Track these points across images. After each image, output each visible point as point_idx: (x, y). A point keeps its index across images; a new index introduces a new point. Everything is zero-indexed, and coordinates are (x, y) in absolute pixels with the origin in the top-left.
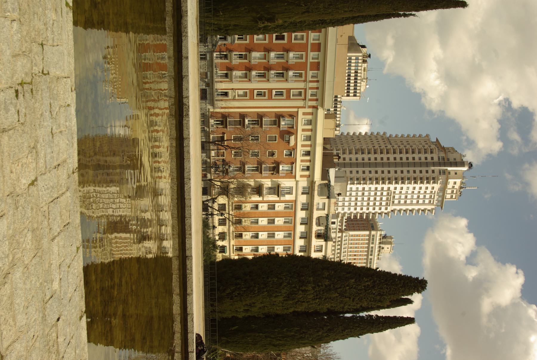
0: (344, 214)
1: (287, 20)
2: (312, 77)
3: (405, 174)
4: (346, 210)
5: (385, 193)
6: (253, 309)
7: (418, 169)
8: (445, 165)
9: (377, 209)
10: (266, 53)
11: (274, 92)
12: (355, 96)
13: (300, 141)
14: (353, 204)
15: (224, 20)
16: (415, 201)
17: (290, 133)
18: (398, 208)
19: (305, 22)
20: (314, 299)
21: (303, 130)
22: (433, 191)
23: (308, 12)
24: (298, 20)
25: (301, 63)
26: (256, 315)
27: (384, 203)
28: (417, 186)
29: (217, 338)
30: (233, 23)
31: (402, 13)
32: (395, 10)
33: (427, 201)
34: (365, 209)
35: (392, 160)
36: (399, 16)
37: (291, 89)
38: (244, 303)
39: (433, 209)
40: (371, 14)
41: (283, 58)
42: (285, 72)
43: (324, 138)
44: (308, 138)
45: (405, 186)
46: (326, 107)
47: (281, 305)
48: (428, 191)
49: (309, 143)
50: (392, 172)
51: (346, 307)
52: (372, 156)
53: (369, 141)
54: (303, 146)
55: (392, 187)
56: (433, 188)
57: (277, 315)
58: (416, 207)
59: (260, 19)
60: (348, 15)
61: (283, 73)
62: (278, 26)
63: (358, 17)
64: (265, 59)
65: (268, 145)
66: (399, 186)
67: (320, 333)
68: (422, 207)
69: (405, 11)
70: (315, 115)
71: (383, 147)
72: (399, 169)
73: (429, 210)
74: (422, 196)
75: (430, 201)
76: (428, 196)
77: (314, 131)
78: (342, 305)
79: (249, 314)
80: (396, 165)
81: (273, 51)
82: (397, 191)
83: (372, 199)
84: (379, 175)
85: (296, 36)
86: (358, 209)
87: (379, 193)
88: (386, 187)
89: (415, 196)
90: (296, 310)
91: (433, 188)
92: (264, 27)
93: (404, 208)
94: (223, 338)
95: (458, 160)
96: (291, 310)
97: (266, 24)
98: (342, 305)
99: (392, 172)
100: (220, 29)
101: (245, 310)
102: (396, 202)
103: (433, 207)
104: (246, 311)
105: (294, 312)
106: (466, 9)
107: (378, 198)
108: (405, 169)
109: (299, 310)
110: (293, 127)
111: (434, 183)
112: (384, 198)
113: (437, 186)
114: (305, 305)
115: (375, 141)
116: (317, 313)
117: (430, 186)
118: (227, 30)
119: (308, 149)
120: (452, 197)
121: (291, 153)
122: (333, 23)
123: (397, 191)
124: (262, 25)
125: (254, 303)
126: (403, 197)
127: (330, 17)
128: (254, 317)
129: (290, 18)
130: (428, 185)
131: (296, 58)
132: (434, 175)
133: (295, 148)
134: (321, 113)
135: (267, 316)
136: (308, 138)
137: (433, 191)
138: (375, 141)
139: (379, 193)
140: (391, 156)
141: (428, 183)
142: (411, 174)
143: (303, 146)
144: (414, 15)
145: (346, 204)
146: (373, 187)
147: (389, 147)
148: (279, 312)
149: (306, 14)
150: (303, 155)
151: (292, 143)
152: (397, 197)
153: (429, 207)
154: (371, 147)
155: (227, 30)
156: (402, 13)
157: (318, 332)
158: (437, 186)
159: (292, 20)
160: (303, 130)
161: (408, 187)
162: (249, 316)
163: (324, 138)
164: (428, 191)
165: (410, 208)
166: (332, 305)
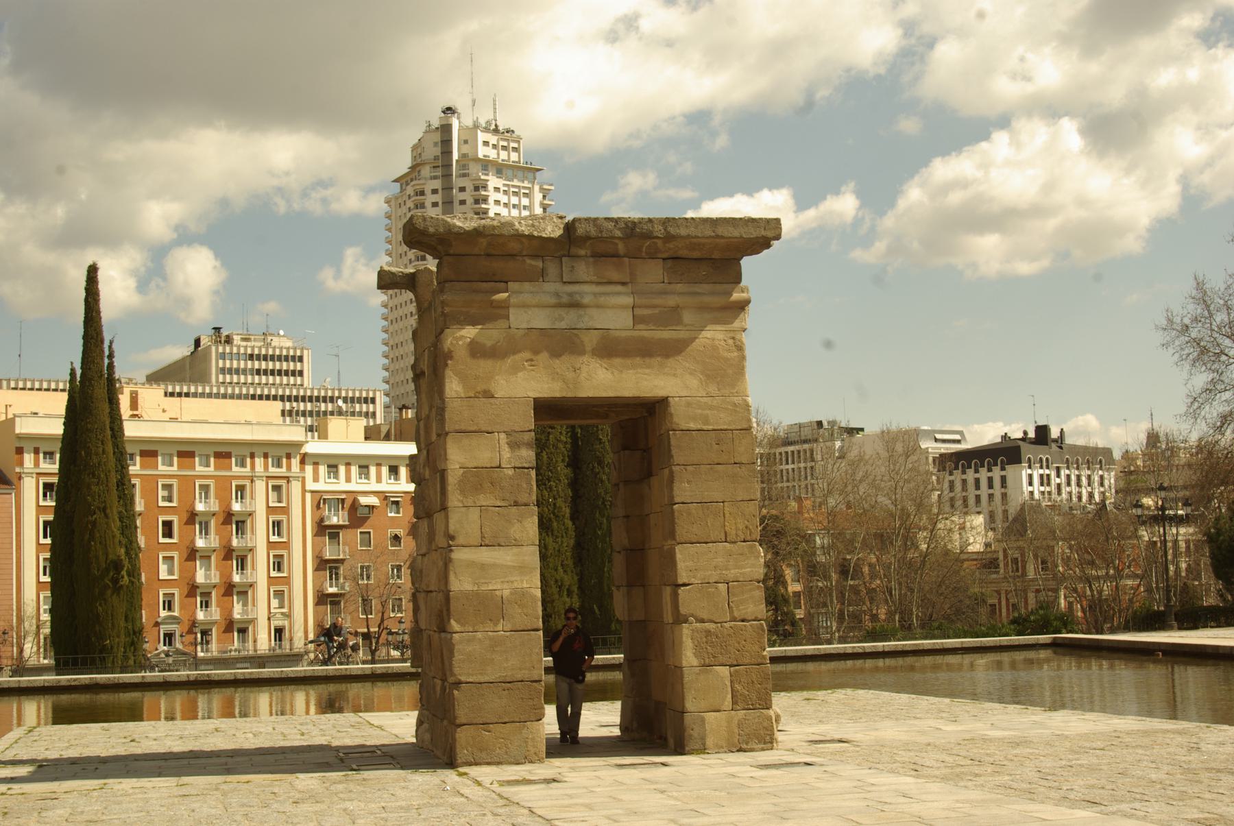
1: (117, 541)
2: (243, 465)
6: (567, 583)
8: (448, 166)
10: (198, 555)
11: (274, 539)
12: (301, 359)
15: (118, 637)
17: (355, 506)
19: (120, 513)
20: (550, 488)
21: (348, 480)
22: (503, 188)
23: (104, 509)
24: (118, 523)
25: (216, 488)
26: (576, 578)
29: (611, 638)
30: (122, 624)
31: (106, 361)
32: (102, 375)
33: (525, 202)
36: (111, 366)
37: (268, 507)
38: (556, 596)
39: (541, 189)
40: (108, 410)
41: (207, 524)
42: (234, 519)
43: (366, 438)
44: (364, 469)
46: (302, 438)
47: (559, 540)
48: (504, 199)
49: (373, 470)
51: (563, 438)
53: (401, 324)
54: (379, 480)
56: (497, 189)
57: (579, 546)
59: (115, 581)
60: (110, 448)
61: (237, 523)
62: (127, 553)
63: (112, 429)
64: (209, 557)
65: (376, 548)
67: (604, 477)
69: (103, 359)
70: (316, 460)
73: (544, 197)
75: (526, 195)
76: (514, 200)
77: (348, 460)
78: (561, 446)
79: (575, 589)
81: (193, 542)
85: (164, 499)
90: (568, 515)
91: (497, 189)
92: (129, 575)
94: (613, 627)
96: (569, 523)
97: (124, 573)
98: (561, 446)
100: (133, 643)
101: (568, 595)
103: (537, 188)
104: (570, 593)
105: (572, 518)
106: (100, 265)
109: (568, 511)
110: (343, 500)
111: (485, 187)
113: (493, 181)
114: (560, 502)
115: (400, 312)
116: (574, 484)
117: (493, 196)
118: (134, 633)
119: (385, 470)
120: (515, 149)
121: (393, 502)
122: (123, 467)
124: (126, 578)
125: (556, 581)
127: (113, 473)
128: (580, 580)
129: (114, 537)
130: (491, 200)
131: (206, 497)
132: (469, 186)
133: (384, 496)
134: (314, 447)
135: (579, 560)
136: (364, 469)
137: (503, 188)
138: (400, 312)
141: (485, 200)
143: (379, 480)
144: (111, 342)
148: (572, 542)
149: (108, 511)
150: (397, 479)
151: (373, 501)
153: (538, 197)
155: (134, 633)
156: (106, 361)
157: (602, 481)
158: (493, 181)
159: (117, 533)
160: (348, 480)
162: (579, 588)
163: (366, 438)
164: (504, 199)
166: (560, 460)
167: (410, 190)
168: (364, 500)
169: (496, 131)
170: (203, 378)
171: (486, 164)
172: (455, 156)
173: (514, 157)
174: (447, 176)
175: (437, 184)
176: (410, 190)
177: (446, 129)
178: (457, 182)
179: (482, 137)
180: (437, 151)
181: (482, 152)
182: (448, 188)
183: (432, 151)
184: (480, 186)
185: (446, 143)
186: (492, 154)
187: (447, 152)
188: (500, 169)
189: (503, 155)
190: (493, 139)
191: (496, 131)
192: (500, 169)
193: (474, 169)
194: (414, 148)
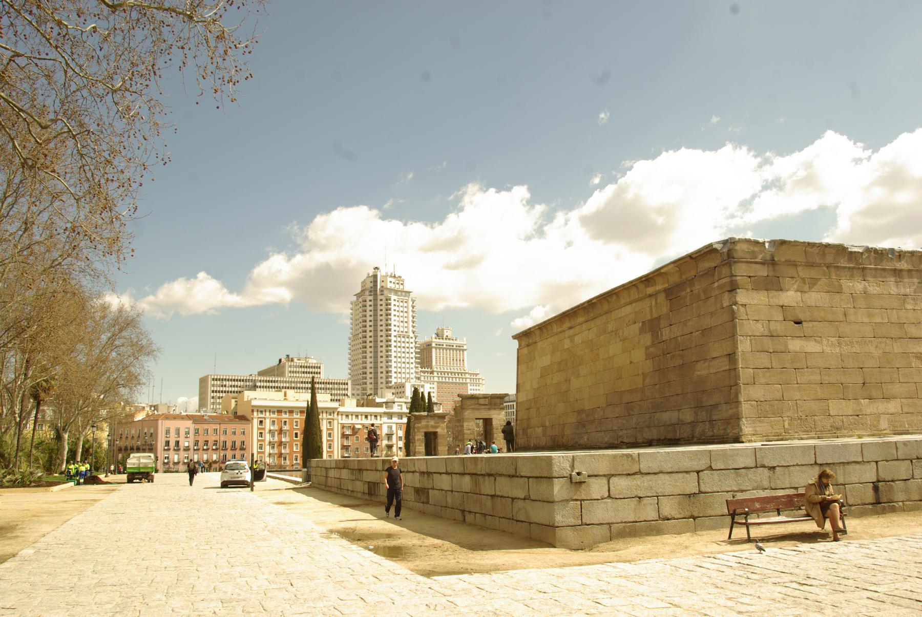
0: (416, 373)
3: (383, 323)
4: (413, 371)
5: (399, 339)
7: (379, 313)
9: (412, 345)
13: (359, 422)
14: (407, 365)
16: (406, 315)
17: (354, 428)
18: (411, 328)
27: (407, 340)
28: (393, 313)
33: (406, 305)
34: (413, 356)
35: (371, 334)
45: (393, 323)
50: (381, 333)
52: (368, 350)
55: (393, 333)
58: (411, 313)
66: (393, 328)
68: (411, 308)
71: (361, 341)
72: (379, 328)
74: (401, 309)
76: (401, 304)
80: (376, 331)
82: (397, 329)
83: (403, 350)
84: (384, 344)
86: (412, 361)
87: (399, 344)
88: (393, 339)
89: (401, 314)
93: (411, 323)
95: (372, 279)
99: (381, 333)
102: (406, 330)
107: (403, 345)
108: (379, 323)
112: (403, 340)
113: (393, 297)
117: (393, 303)
123: (397, 329)
126: (402, 324)
133: (363, 425)
139: (399, 344)
140: (369, 334)
142: (383, 318)
145: (408, 371)
146: (393, 349)
147: (360, 336)
151: (360, 427)
152: (402, 329)
153: (410, 303)
154: (361, 351)
158: (393, 297)
161: (394, 321)
165: (411, 319)
167: (360, 300)
168: (357, 426)
169: (395, 277)
170: (282, 374)
171: (391, 290)
172: (379, 287)
173: (401, 287)
174: (375, 295)
175: (371, 298)
176: (360, 300)
177: (375, 276)
178: (379, 297)
179: (389, 279)
180: (372, 285)
181: (389, 285)
182: (375, 299)
183: (369, 285)
184: (388, 299)
185: (375, 282)
186: (392, 286)
187: (376, 285)
188: (396, 292)
189: (397, 286)
190: (393, 280)
191: (395, 277)
192: (396, 292)
193: (386, 292)
194: (362, 283)
